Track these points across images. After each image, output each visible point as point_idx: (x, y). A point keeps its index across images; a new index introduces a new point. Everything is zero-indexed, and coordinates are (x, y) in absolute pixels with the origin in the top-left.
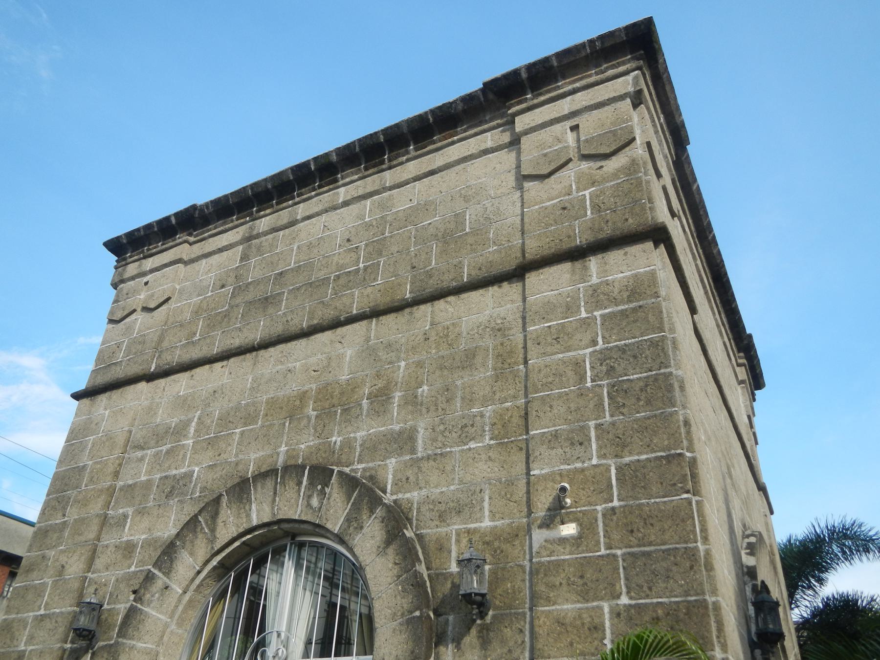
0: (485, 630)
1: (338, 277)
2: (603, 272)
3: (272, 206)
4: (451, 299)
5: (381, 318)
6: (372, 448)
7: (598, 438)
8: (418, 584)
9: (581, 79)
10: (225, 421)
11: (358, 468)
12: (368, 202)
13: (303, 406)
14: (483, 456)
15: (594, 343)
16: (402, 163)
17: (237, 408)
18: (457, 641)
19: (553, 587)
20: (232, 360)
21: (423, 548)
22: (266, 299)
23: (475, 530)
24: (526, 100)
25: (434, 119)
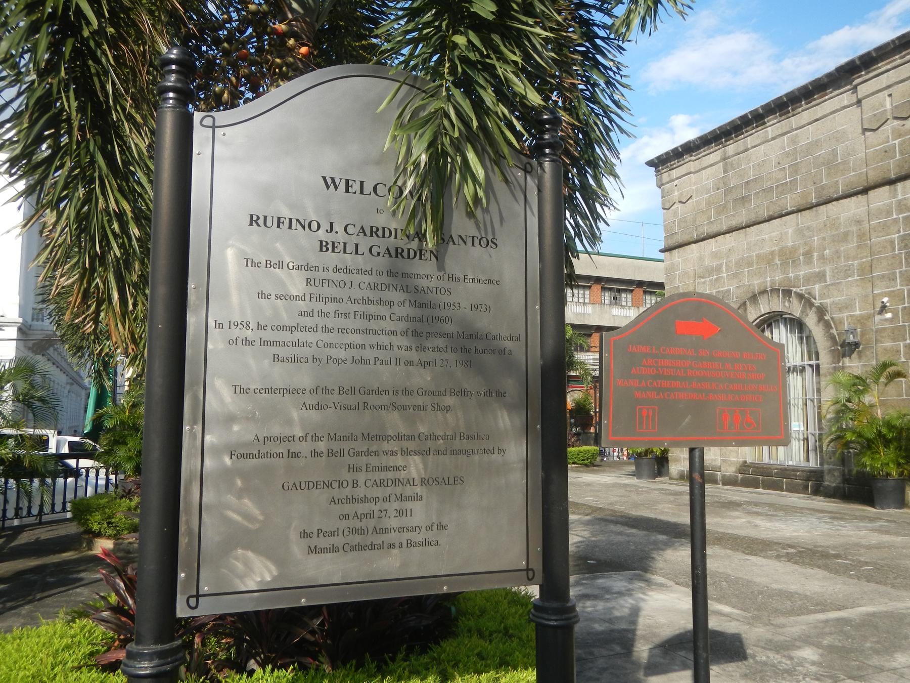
0: (860, 352)
1: (777, 186)
2: (904, 193)
3: (732, 139)
4: (834, 203)
5: (803, 212)
6: (808, 280)
7: (900, 277)
8: (832, 338)
9: (891, 62)
10: (739, 264)
11: (802, 289)
12: (785, 137)
13: (773, 259)
14: (855, 284)
15: (899, 232)
16: (799, 113)
17: (743, 259)
18: (850, 356)
19: (882, 337)
20: (734, 233)
21: (834, 322)
22: (743, 197)
23: (853, 316)
24: (861, 76)
25: (813, 87)
